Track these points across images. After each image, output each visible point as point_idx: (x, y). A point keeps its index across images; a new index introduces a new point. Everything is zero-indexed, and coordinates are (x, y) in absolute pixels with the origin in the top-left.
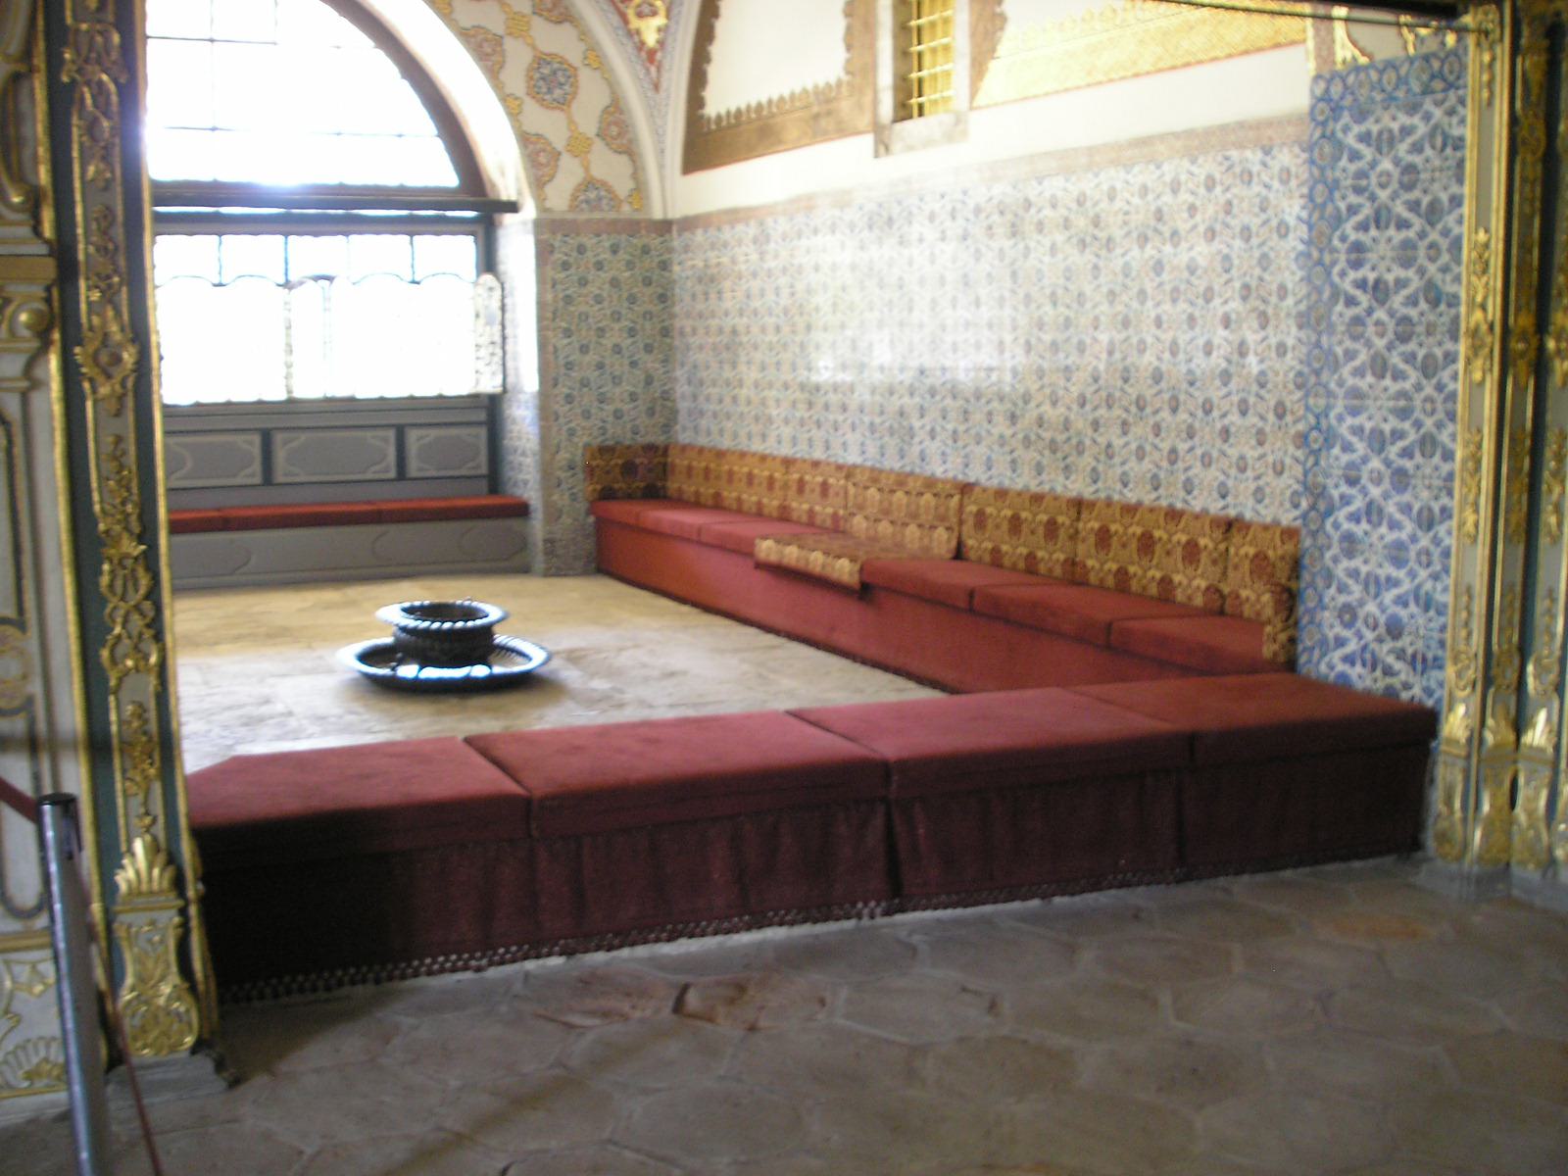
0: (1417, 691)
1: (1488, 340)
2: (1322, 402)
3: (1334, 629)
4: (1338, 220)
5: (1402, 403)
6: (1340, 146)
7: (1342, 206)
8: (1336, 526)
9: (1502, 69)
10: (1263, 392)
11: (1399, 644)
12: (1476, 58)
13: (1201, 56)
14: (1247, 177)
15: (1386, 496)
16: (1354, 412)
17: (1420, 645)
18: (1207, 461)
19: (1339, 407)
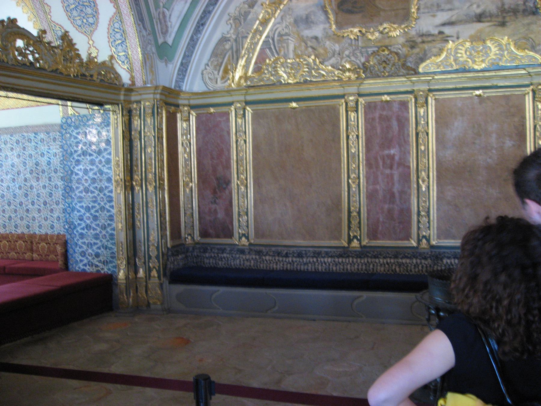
0: (106, 270)
1: (121, 183)
2: (70, 200)
3: (78, 257)
4: (72, 154)
5: (94, 199)
6: (71, 135)
7: (73, 151)
8: (77, 231)
9: (120, 120)
10: (39, 199)
11: (99, 259)
12: (112, 116)
13: (12, 107)
14: (30, 140)
15: (92, 222)
16: (80, 202)
17: (105, 258)
18: (22, 219)
19: (76, 201)
